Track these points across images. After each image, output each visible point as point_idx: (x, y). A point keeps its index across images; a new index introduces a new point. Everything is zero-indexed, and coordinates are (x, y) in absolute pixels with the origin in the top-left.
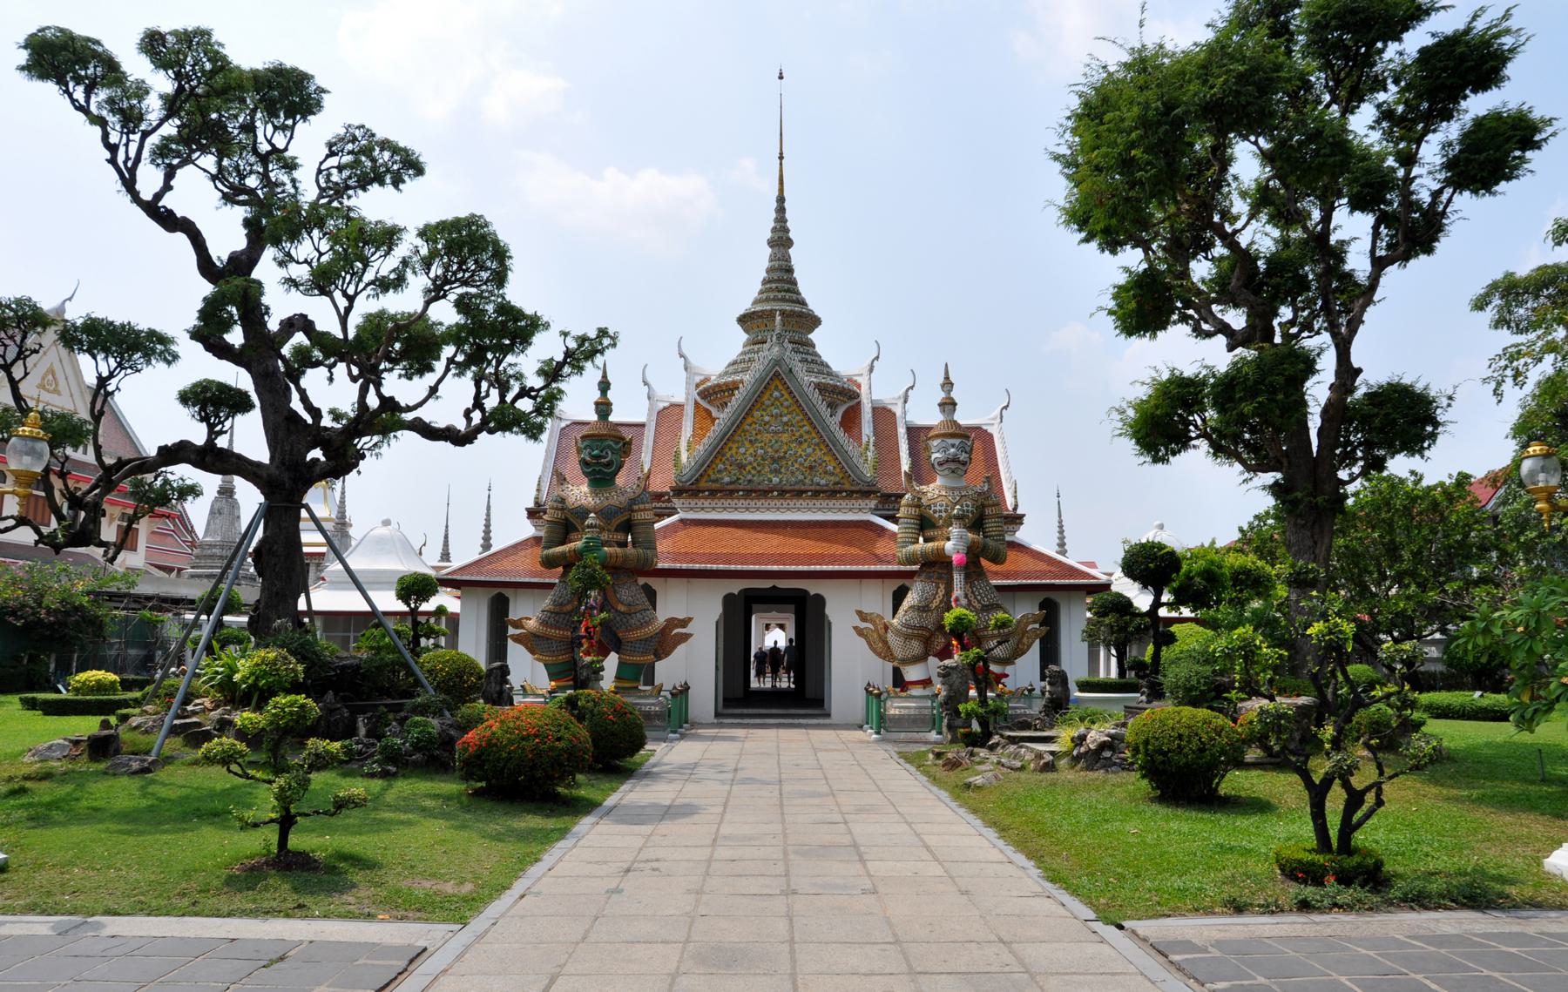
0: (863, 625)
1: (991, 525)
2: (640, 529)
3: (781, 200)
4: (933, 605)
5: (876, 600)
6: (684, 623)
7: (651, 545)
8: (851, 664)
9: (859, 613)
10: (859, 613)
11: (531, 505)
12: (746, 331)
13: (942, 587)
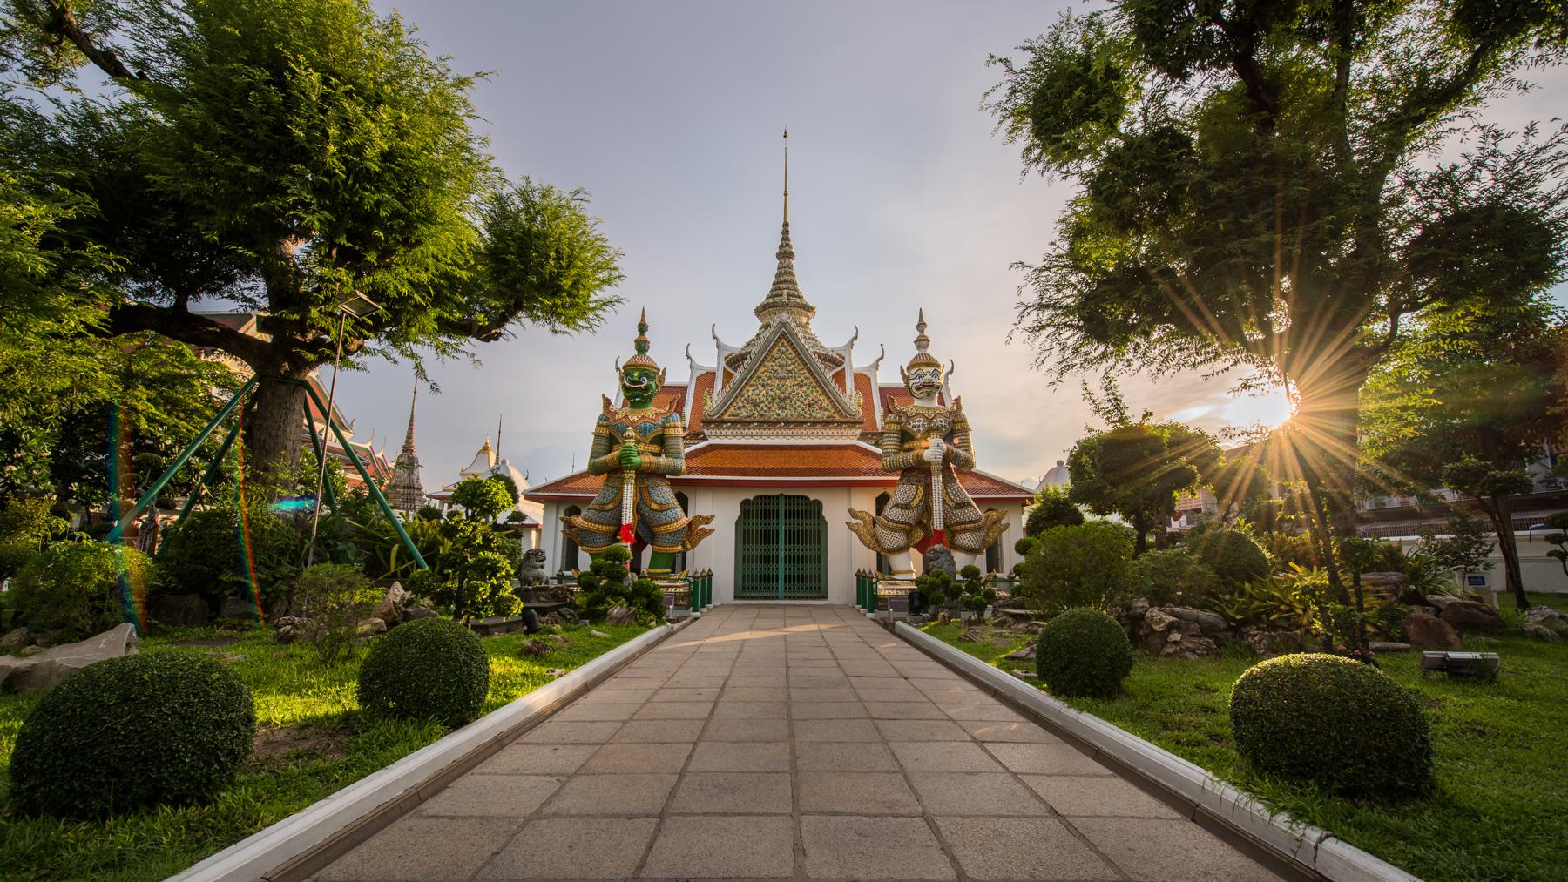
0: (854, 521)
2: (670, 442)
3: (786, 225)
6: (708, 520)
8: (845, 552)
9: (851, 511)
10: (851, 511)
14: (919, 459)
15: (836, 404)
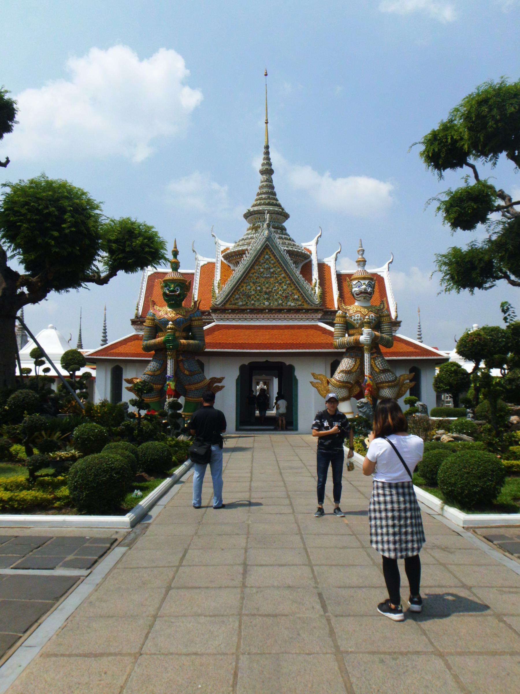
0: (315, 381)
1: (385, 327)
4: (354, 370)
5: (321, 369)
6: (220, 380)
7: (202, 339)
9: (313, 375)
11: (133, 317)
12: (249, 222)
13: (358, 360)
14: (357, 342)
15: (305, 297)
